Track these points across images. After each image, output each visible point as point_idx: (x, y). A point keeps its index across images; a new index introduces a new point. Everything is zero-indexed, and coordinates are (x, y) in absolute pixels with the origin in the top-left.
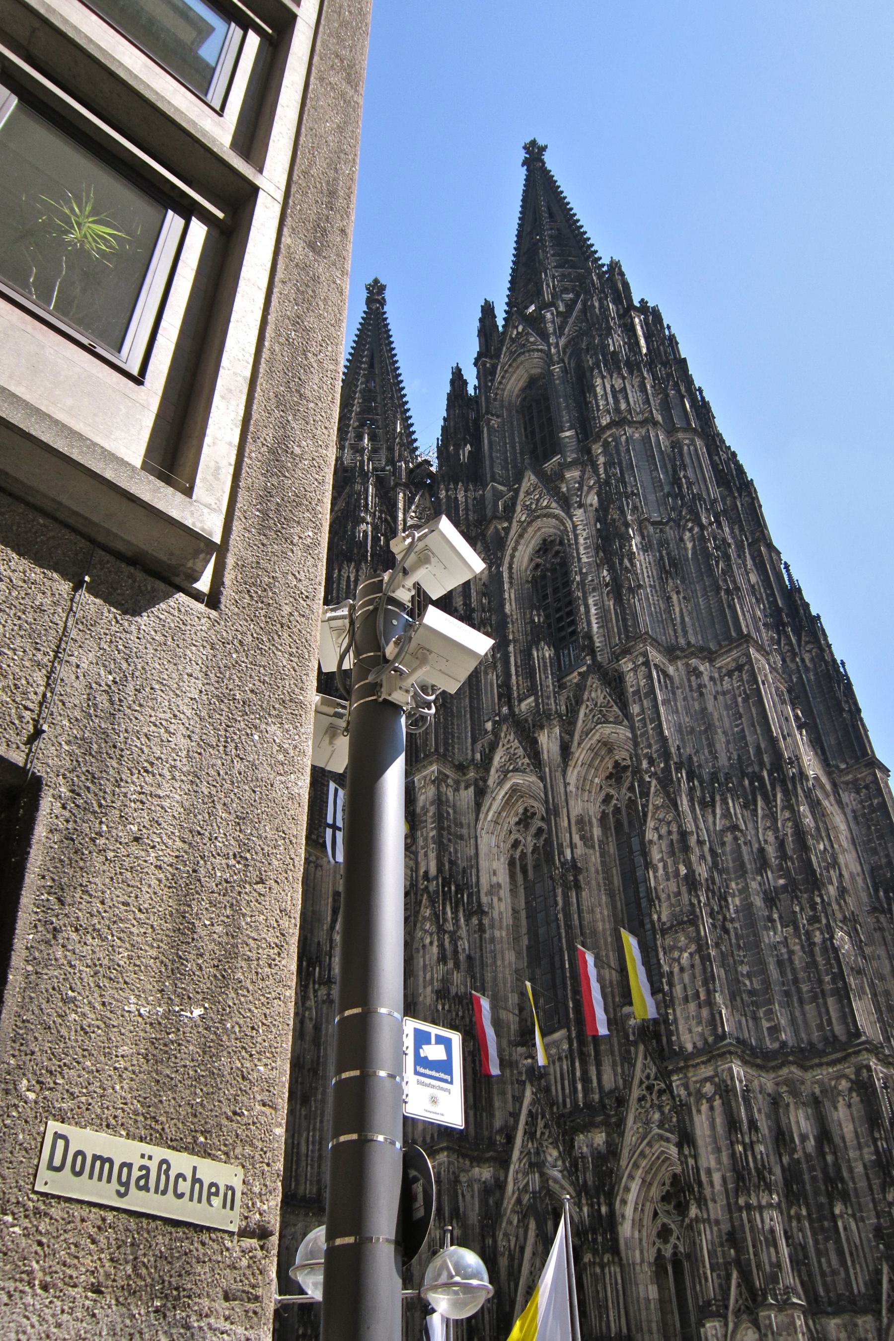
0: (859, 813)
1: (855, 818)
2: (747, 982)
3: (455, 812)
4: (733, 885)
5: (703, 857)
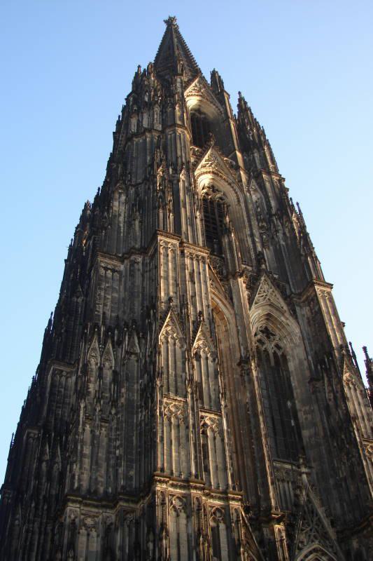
0: (311, 318)
1: (309, 322)
2: (117, 452)
3: (65, 390)
4: (123, 390)
5: (100, 376)
